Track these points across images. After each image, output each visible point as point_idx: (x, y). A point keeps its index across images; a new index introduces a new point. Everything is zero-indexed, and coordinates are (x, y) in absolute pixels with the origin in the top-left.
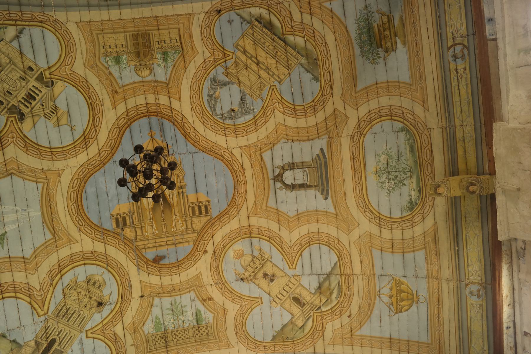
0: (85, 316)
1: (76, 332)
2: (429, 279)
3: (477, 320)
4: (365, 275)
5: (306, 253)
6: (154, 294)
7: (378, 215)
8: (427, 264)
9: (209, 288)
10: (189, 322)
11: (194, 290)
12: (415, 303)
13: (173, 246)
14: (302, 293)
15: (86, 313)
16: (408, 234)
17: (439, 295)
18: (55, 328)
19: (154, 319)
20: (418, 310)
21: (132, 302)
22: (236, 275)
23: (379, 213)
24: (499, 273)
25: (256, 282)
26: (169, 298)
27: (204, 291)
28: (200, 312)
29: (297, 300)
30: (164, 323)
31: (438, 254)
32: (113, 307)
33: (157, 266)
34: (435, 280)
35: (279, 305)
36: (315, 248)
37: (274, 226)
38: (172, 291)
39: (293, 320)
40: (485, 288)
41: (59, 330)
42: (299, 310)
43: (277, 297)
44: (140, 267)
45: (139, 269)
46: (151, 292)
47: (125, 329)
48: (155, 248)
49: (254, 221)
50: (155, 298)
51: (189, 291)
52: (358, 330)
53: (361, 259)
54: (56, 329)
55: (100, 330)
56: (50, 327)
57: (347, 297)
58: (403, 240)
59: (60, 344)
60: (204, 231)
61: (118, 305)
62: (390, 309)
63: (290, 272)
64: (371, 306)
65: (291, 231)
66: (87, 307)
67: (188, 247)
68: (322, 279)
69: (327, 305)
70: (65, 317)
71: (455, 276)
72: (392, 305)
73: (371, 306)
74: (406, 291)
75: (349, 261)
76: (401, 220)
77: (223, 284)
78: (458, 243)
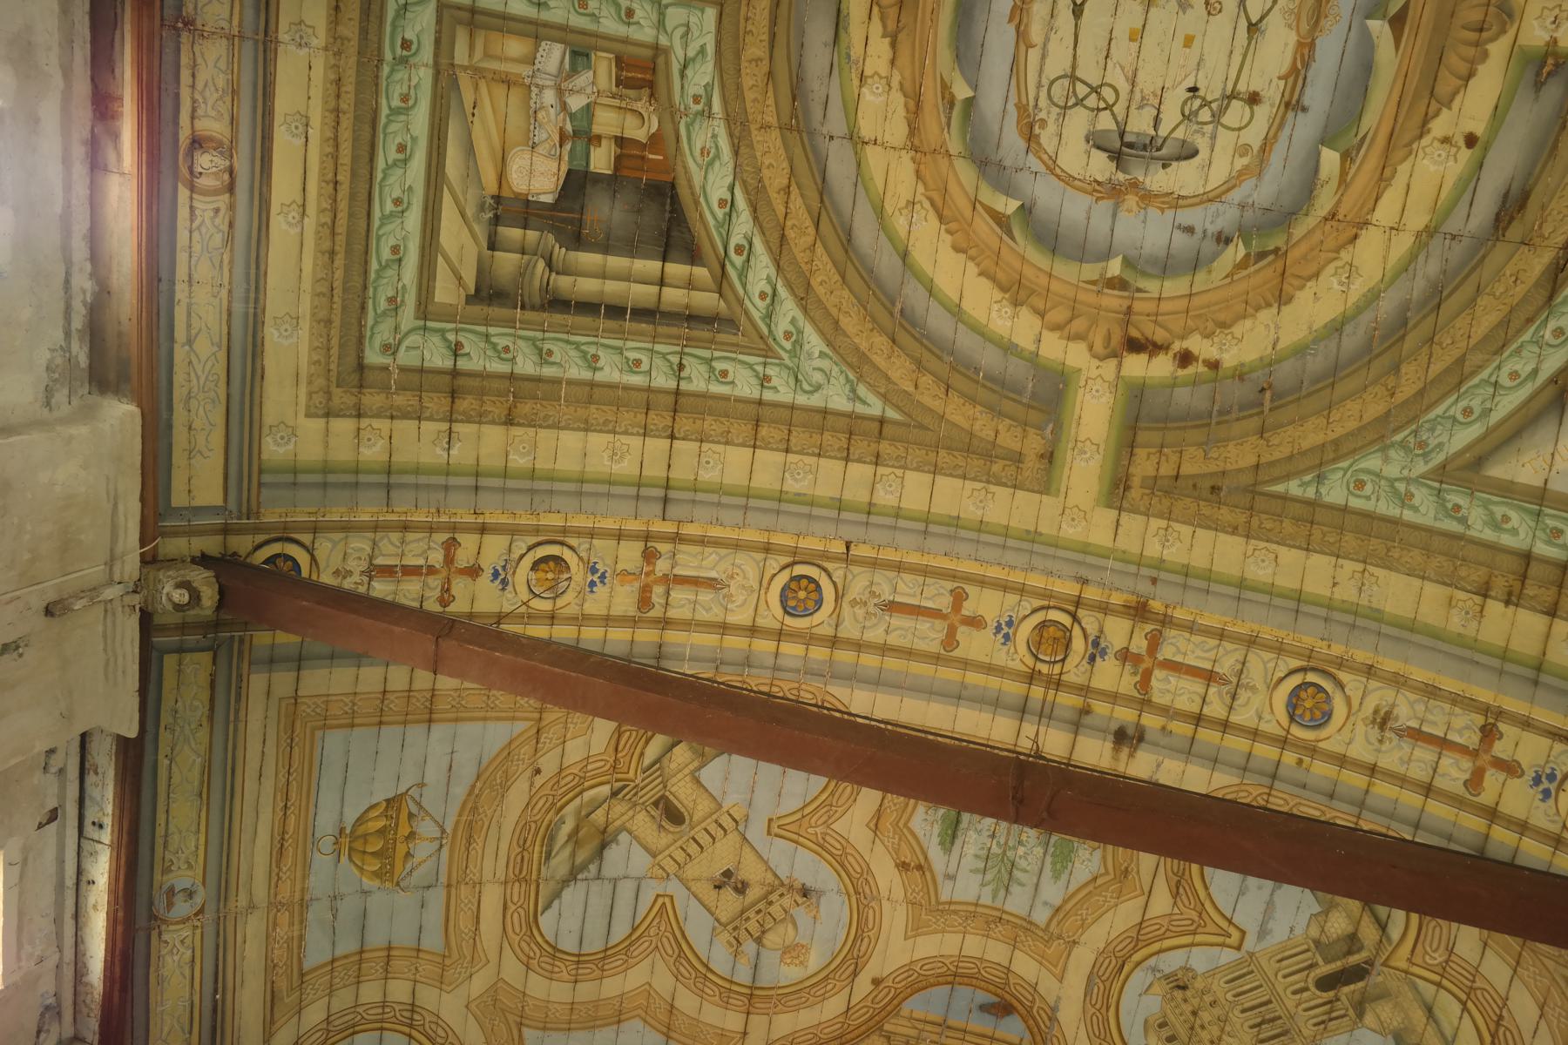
0: (1227, 982)
1: (1264, 963)
2: (302, 900)
3: (180, 832)
4: (474, 883)
5: (620, 931)
6: (1041, 934)
7: (414, 1033)
8: (301, 938)
9: (898, 893)
10: (979, 827)
11: (938, 903)
12: (348, 831)
13: (950, 1022)
14: (656, 834)
15: (1219, 987)
16: (343, 999)
17: (278, 866)
18: (1306, 1010)
19: (1064, 877)
20: (342, 813)
21: (1102, 946)
22: (818, 907)
23: (410, 1036)
24: (112, 972)
25: (770, 877)
26: (1007, 908)
27: (914, 891)
28: (941, 843)
29: (673, 815)
30: (1045, 854)
31: (270, 967)
32: (1152, 961)
33: (1007, 997)
34: (284, 901)
35: (725, 809)
36: (594, 945)
37: (687, 1002)
38: (993, 920)
39: (696, 764)
40: (153, 917)
41: (1298, 996)
42: (673, 790)
43: (725, 831)
44: (1049, 1012)
45: (1054, 1009)
46: (1047, 942)
47: (1147, 894)
48: (996, 1036)
49: (733, 1021)
50: (1042, 925)
51: (950, 903)
52: (520, 735)
53: (478, 922)
54: (1304, 1006)
55: (1206, 930)
56: (1315, 1020)
57: (533, 826)
58: (358, 982)
59: (1311, 966)
60: (863, 1028)
61: (1137, 957)
62: (419, 804)
63: (674, 887)
64: (469, 806)
65: (647, 987)
66: (1212, 999)
67: (915, 1006)
68: (593, 868)
69: (592, 800)
70: (1272, 1015)
71: (230, 929)
72: (411, 816)
73: (472, 805)
74: (368, 858)
75: (508, 917)
76: (357, 1028)
77: (857, 893)
78: (215, 1010)
